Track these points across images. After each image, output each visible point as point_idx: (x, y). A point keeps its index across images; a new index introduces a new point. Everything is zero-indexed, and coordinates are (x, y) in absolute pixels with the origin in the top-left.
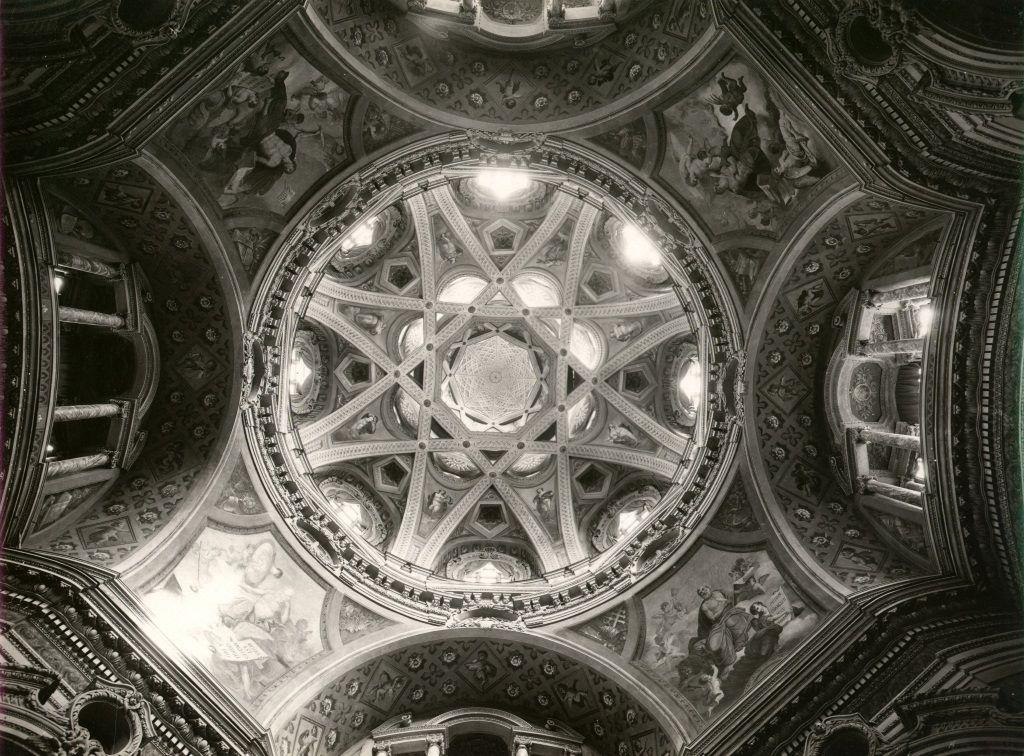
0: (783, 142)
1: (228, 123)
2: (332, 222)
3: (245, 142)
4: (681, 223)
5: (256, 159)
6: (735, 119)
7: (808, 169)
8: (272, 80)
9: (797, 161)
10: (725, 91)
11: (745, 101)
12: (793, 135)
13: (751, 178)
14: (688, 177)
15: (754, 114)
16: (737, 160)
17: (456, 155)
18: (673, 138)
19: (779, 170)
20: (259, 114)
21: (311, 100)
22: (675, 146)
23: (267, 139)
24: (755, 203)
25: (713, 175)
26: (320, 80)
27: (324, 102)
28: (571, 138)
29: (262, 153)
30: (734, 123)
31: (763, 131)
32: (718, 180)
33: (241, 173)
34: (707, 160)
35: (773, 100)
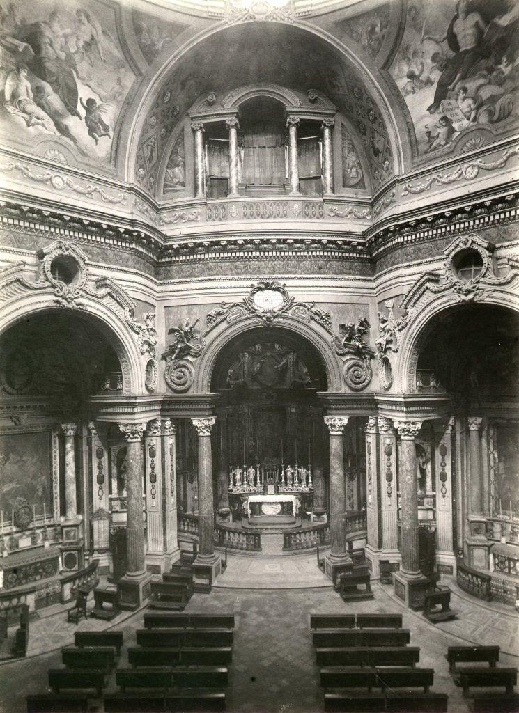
0: (39, 105)
1: (490, 83)
3: (486, 56)
5: (486, 30)
6: (81, 99)
8: (441, 108)
9: (18, 97)
10: (101, 122)
11: (84, 120)
12: (38, 118)
13: (37, 49)
14: (88, 17)
18: (117, 53)
19: (24, 74)
20: (463, 78)
21: (420, 75)
22: (113, 46)
23: (469, 48)
24: (19, 23)
26: (407, 93)
27: (411, 69)
28: (203, 21)
30: (80, 95)
34: (81, 43)
35: (67, 140)
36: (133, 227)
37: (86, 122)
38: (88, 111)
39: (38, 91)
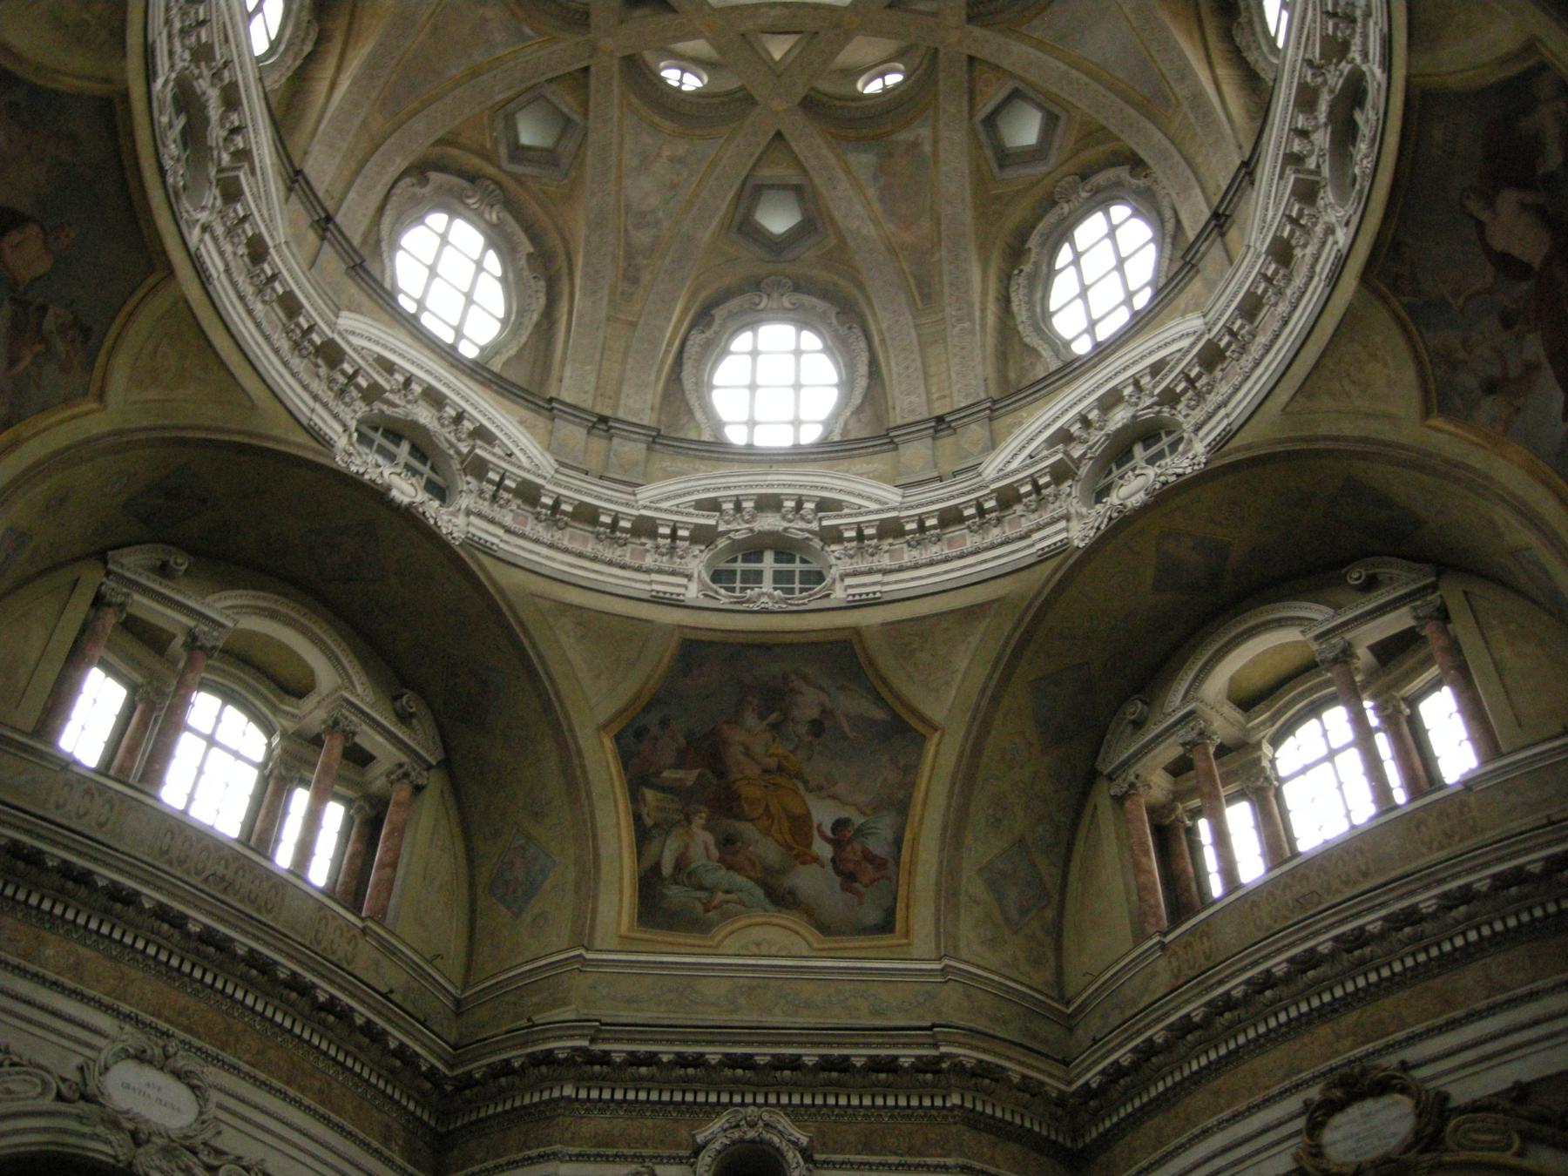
0: (730, 868)
2: (1335, 79)
4: (749, 601)
6: (819, 826)
7: (667, 869)
10: (869, 857)
11: (829, 868)
12: (727, 892)
14: (805, 678)
15: (804, 863)
16: (765, 771)
17: (1199, 376)
19: (699, 820)
25: (774, 717)
29: (1540, 211)
30: (816, 819)
31: (768, 850)
32: (762, 717)
33: (1553, 159)
34: (803, 729)
36: (936, 1046)
37: (838, 871)
38: (838, 843)
39: (727, 842)
